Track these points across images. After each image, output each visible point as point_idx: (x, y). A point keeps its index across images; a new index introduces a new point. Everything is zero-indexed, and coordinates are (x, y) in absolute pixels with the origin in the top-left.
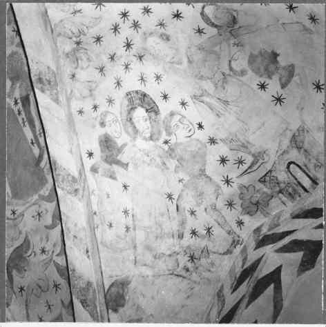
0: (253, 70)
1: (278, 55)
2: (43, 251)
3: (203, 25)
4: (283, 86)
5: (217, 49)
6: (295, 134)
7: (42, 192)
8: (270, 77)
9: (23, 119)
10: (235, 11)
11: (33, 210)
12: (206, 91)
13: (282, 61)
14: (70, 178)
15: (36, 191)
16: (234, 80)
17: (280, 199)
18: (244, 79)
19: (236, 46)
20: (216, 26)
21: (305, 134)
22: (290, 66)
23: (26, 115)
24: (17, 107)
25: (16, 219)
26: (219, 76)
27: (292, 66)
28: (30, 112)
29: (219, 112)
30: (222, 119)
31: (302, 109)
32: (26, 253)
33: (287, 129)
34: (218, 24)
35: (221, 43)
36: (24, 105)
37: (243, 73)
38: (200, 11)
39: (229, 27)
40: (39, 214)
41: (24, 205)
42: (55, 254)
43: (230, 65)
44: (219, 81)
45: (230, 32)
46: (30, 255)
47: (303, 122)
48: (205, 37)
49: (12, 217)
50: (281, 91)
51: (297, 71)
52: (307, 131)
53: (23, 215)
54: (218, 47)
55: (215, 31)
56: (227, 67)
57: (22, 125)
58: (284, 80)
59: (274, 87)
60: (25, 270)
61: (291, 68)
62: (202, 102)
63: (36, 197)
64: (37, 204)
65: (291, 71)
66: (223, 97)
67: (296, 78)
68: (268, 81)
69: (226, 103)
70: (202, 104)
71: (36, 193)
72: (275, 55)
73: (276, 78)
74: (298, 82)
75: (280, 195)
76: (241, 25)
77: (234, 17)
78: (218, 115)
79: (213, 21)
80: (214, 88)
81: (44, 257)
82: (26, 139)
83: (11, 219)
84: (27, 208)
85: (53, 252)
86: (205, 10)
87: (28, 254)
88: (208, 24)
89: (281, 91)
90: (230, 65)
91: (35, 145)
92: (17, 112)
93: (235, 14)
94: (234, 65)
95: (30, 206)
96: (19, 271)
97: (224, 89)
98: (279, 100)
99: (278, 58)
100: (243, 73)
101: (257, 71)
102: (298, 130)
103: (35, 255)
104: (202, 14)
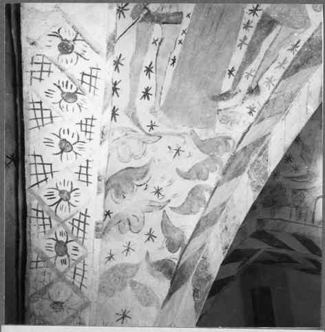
2: (158, 192)
7: (197, 131)
9: (245, 38)
11: (175, 142)
14: (263, 173)
15: (192, 123)
17: (291, 210)
23: (252, 38)
24: (251, 17)
25: (150, 135)
28: (259, 42)
32: (138, 180)
36: (260, 25)
40: (178, 151)
41: (170, 127)
42: (169, 205)
46: (141, 185)
49: (147, 129)
53: (161, 137)
57: (239, 42)
60: (124, 197)
63: (187, 130)
64: (184, 137)
71: (191, 127)
75: (294, 209)
81: (155, 197)
82: (229, 61)
83: (143, 130)
84: (172, 134)
85: (169, 201)
87: (138, 183)
91: (232, 78)
92: (244, 21)
95: (172, 134)
96: (117, 194)
103: (146, 188)
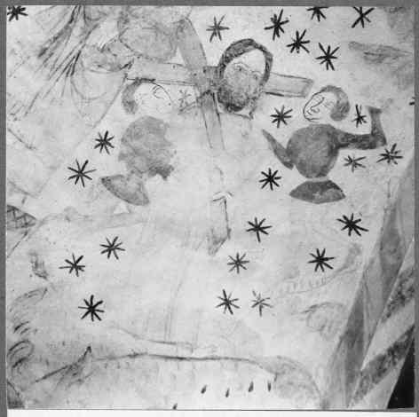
0: (134, 125)
1: (165, 177)
3: (229, 38)
4: (105, 181)
5: (178, 59)
6: (18, 210)
8: (122, 157)
10: (250, 113)
12: (96, 26)
13: (153, 184)
16: (116, 87)
18: (118, 107)
19: (180, 96)
20: (223, 66)
21: (20, 230)
22: (145, 196)
26: (124, 55)
27: (146, 202)
29: (51, 55)
30: (34, 61)
31: (68, 219)
33: (26, 193)
34: (226, 70)
35: (189, 67)
37: (130, 105)
38: (259, 41)
39: (220, 90)
43: (146, 80)
44: (115, 55)
45: (208, 92)
47: (43, 222)
48: (204, 37)
50: (96, 177)
51: (137, 209)
52: (26, 234)
54: (182, 62)
55: (214, 61)
56: (140, 75)
58: (117, 183)
59: (105, 164)
61: (142, 198)
62: (72, 20)
65: (137, 198)
66: (82, 63)
67: (123, 206)
68: (115, 152)
69: (70, 70)
70: (68, 18)
72: (164, 172)
73: (122, 168)
74: (117, 212)
76: (221, 116)
77: (238, 109)
78: (43, 52)
79: (235, 60)
80: (101, 44)
86: (261, 53)
88: (228, 49)
89: (96, 177)
90: (146, 80)
93: (245, 111)
94: (145, 88)
97: (99, 66)
98: (80, 174)
99: (158, 177)
100: (130, 105)
101: (132, 133)
102: (25, 215)
104: (250, 43)
